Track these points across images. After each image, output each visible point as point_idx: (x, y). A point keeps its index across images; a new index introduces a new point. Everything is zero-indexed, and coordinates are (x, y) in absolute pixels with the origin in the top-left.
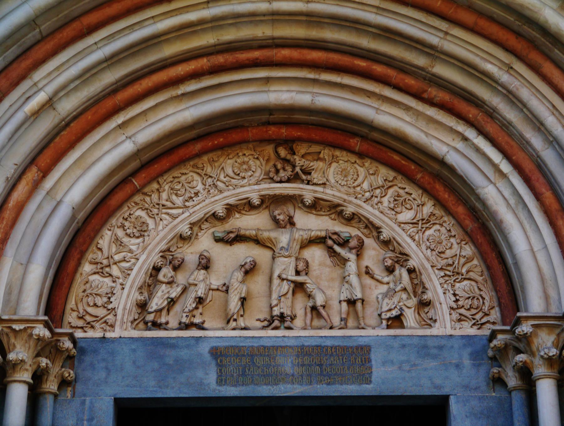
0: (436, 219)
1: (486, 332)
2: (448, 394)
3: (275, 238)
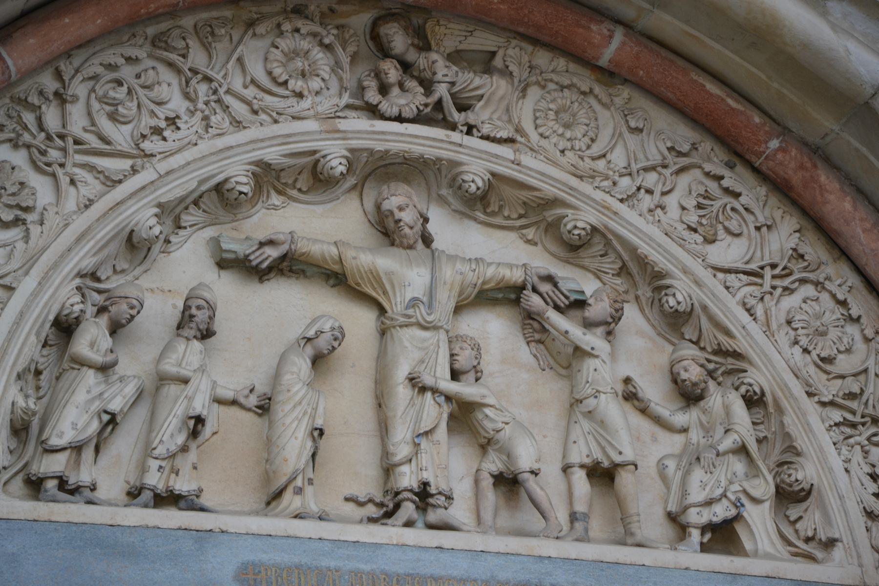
0: (806, 267)
3: (389, 274)
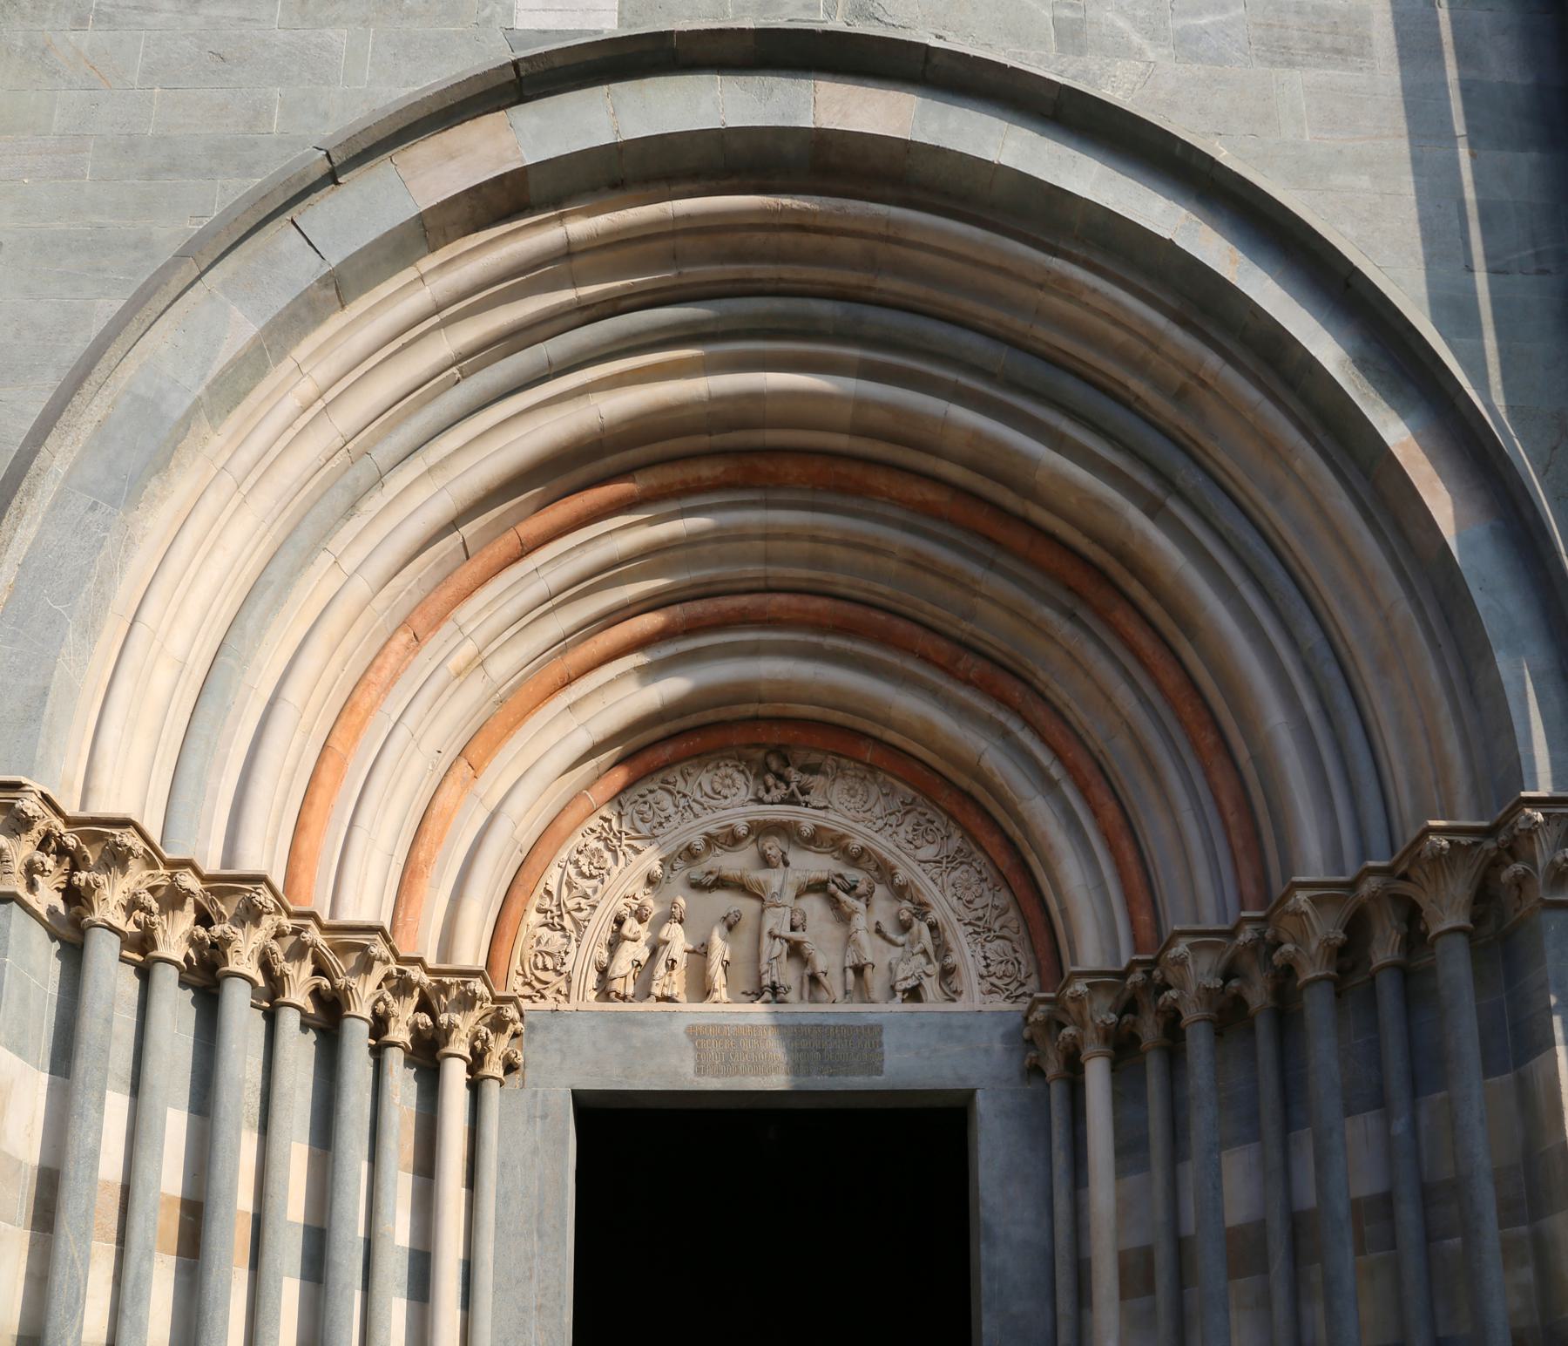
1: (1022, 1006)
3: (765, 882)
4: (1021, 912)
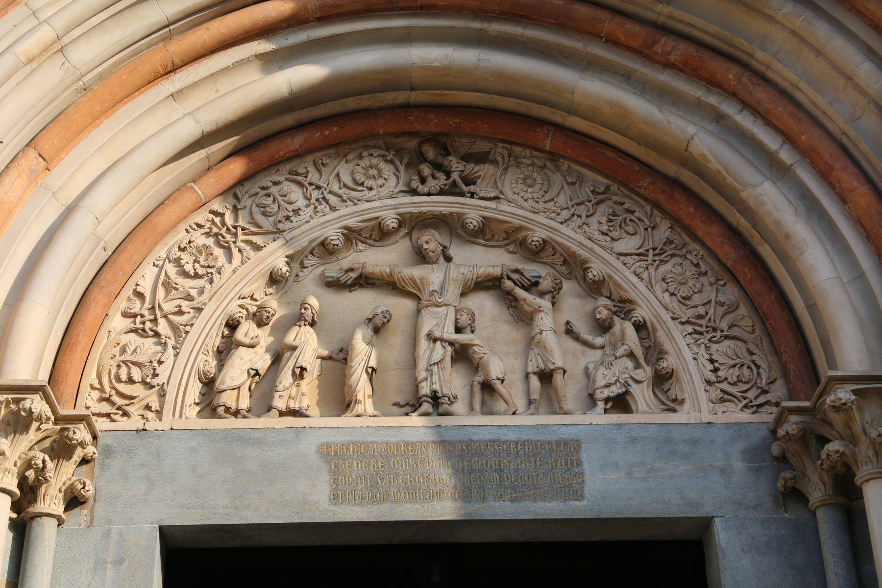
1: (768, 416)
2: (711, 515)
3: (421, 279)
4: (755, 307)
